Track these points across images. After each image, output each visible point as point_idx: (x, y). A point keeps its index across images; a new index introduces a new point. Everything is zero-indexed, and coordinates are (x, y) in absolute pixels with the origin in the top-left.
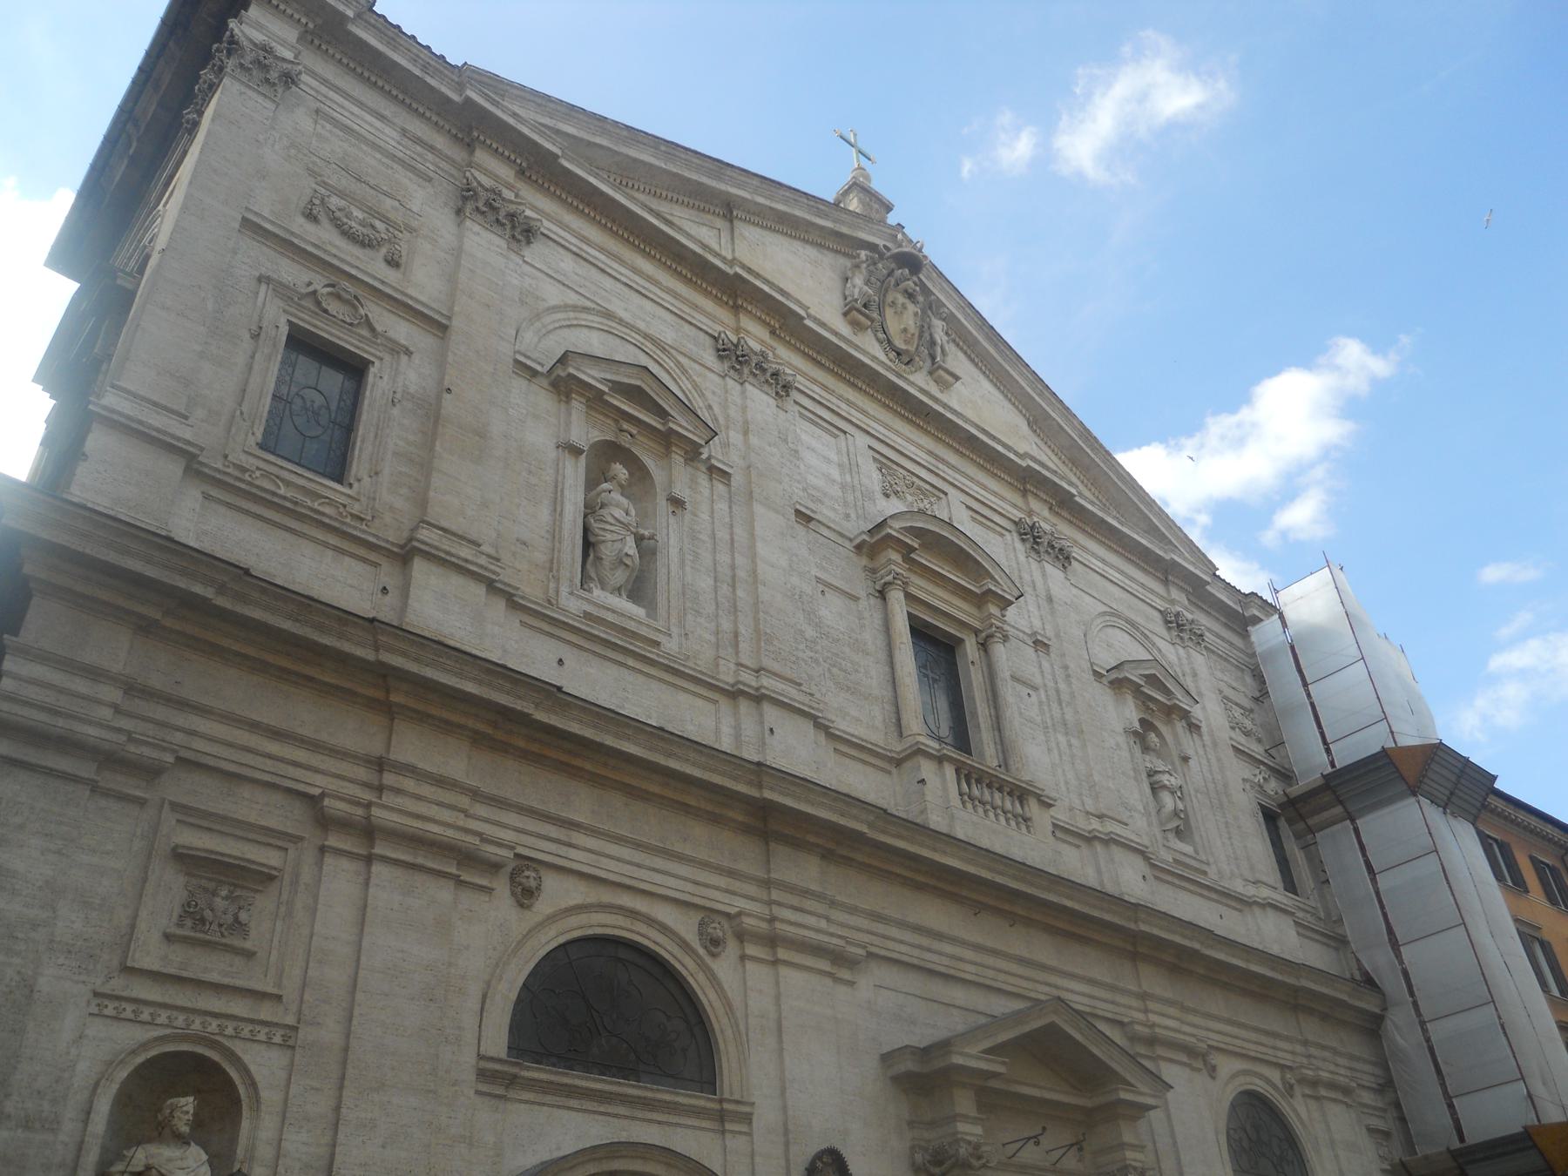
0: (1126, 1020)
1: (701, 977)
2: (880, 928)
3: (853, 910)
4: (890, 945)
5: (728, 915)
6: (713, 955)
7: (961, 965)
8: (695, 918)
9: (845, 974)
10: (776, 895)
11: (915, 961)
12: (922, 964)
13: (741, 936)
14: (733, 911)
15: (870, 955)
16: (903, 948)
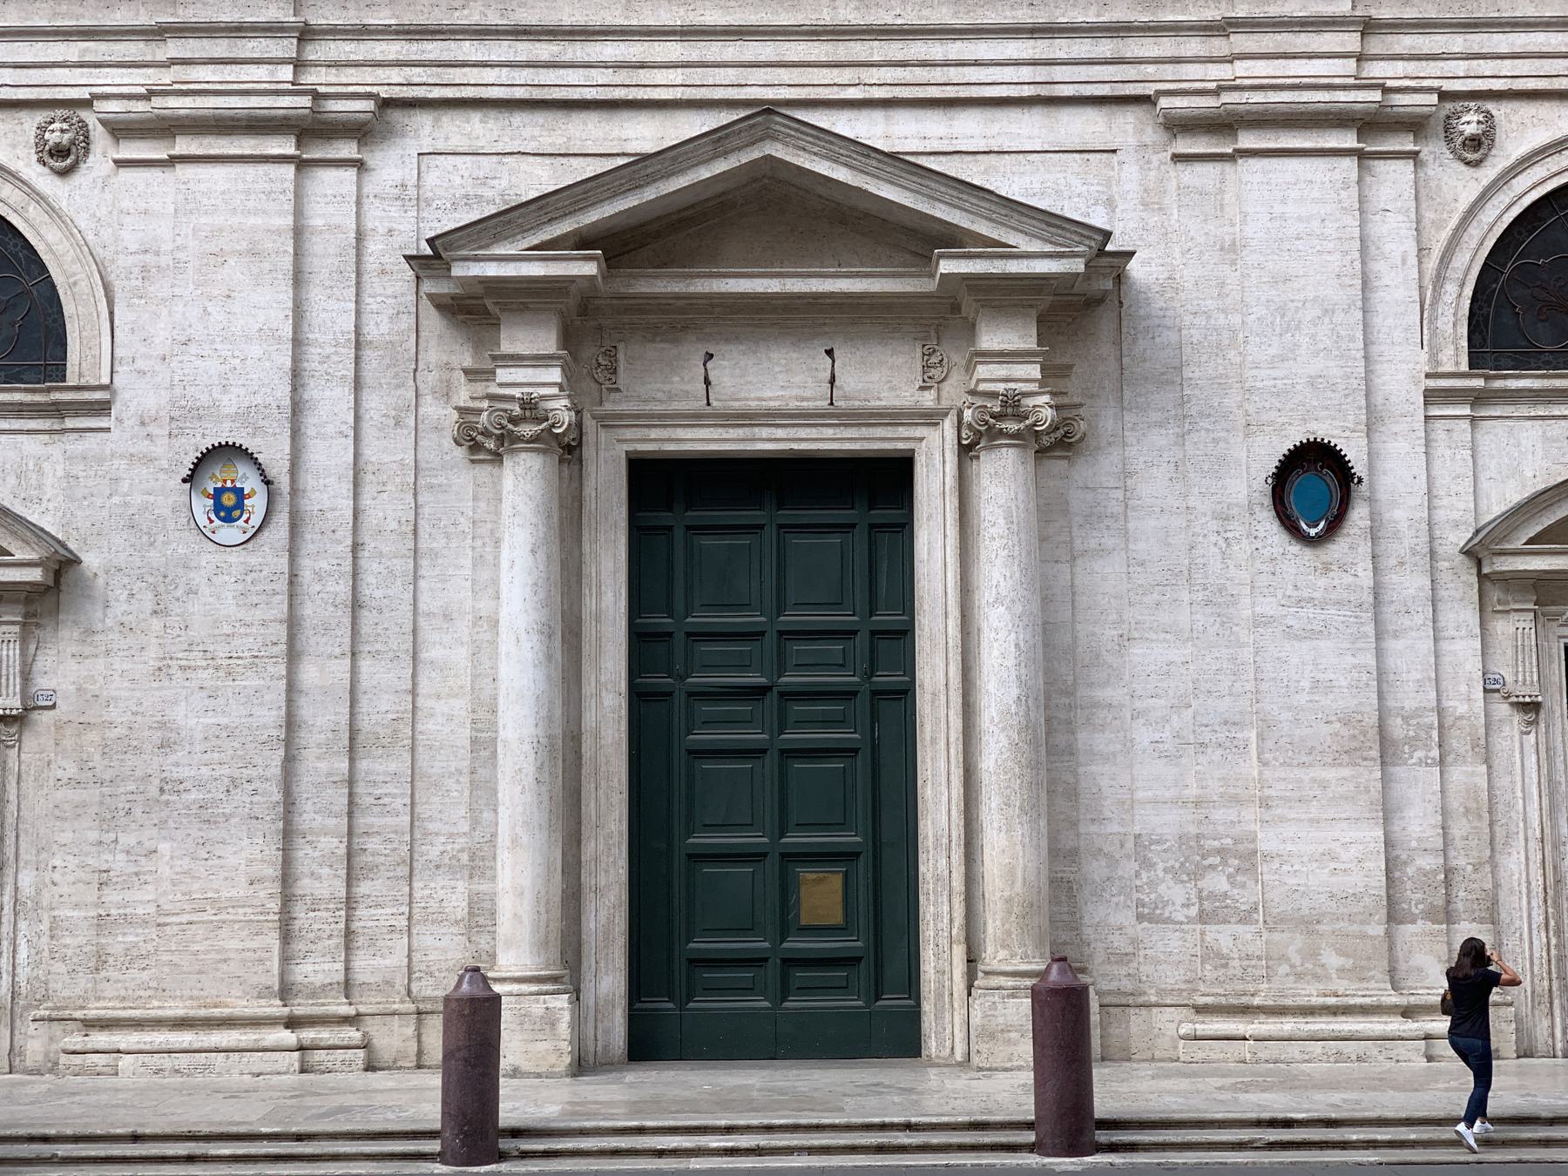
0: (1150, 89)
1: (33, 210)
2: (433, 50)
3: (362, 32)
4: (456, 75)
5: (87, 104)
6: (64, 173)
7: (644, 76)
8: (30, 122)
9: (347, 150)
10: (173, 48)
11: (519, 93)
12: (537, 94)
13: (120, 130)
14: (83, 94)
15: (386, 104)
16: (489, 75)
